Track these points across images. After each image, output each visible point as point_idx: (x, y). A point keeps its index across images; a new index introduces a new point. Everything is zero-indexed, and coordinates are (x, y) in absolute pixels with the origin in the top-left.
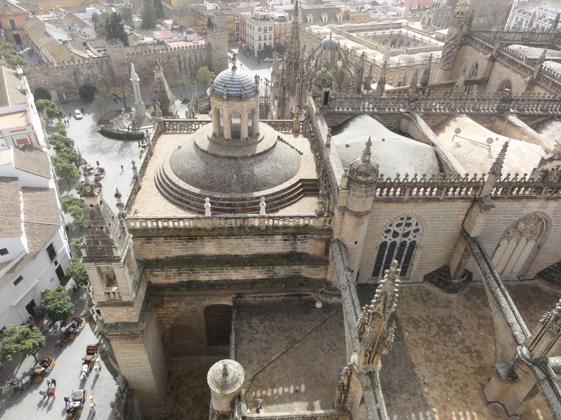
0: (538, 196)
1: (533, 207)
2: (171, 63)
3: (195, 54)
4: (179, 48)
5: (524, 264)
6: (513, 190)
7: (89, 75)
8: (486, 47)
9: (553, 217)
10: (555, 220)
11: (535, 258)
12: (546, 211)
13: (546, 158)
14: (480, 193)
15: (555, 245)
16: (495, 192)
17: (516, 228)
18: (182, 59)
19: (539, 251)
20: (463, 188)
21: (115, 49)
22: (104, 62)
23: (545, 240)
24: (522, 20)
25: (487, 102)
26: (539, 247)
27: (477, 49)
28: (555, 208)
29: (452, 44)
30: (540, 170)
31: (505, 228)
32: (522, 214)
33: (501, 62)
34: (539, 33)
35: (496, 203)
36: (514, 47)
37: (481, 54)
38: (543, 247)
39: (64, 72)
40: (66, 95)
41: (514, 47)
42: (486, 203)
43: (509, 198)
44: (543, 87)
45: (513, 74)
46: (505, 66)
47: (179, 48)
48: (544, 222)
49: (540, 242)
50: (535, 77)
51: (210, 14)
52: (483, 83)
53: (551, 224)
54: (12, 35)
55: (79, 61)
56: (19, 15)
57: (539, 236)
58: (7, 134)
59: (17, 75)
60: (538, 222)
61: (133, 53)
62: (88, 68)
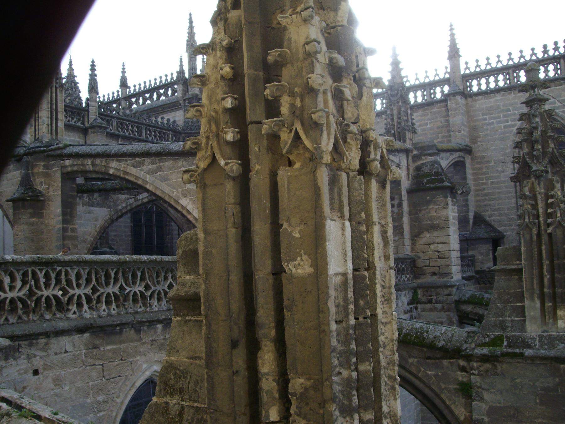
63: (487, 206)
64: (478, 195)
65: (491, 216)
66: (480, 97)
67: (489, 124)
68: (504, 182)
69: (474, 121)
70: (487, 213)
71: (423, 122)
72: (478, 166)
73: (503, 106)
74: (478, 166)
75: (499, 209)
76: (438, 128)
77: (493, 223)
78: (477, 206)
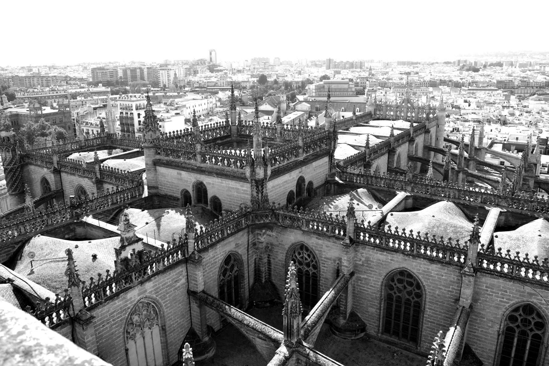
0: (132, 285)
1: (134, 295)
5: (162, 352)
6: (105, 291)
8: (46, 162)
9: (157, 296)
10: (160, 298)
11: (167, 342)
12: (147, 294)
13: (118, 248)
14: (74, 310)
15: (175, 320)
16: (89, 302)
17: (132, 324)
19: (166, 332)
20: (52, 315)
23: (164, 320)
24: (88, 130)
25: (58, 214)
26: (163, 329)
27: (39, 166)
28: (153, 287)
29: (12, 169)
30: (119, 261)
31: (122, 330)
32: (129, 308)
33: (66, 172)
34: (92, 139)
35: (94, 313)
36: (74, 156)
37: (45, 170)
38: (167, 327)
41: (74, 156)
42: (84, 318)
43: (106, 300)
44: (110, 183)
45: (81, 179)
46: (71, 174)
48: (153, 304)
49: (161, 324)
50: (99, 176)
52: (60, 194)
53: (160, 304)
57: (157, 319)
60: (148, 307)
63: (475, 342)
64: (470, 334)
65: (477, 349)
66: (487, 275)
67: (489, 295)
68: (491, 334)
69: (478, 288)
70: (474, 347)
71: (440, 273)
72: (474, 317)
73: (503, 287)
74: (474, 317)
75: (482, 348)
76: (451, 281)
77: (477, 354)
78: (467, 340)
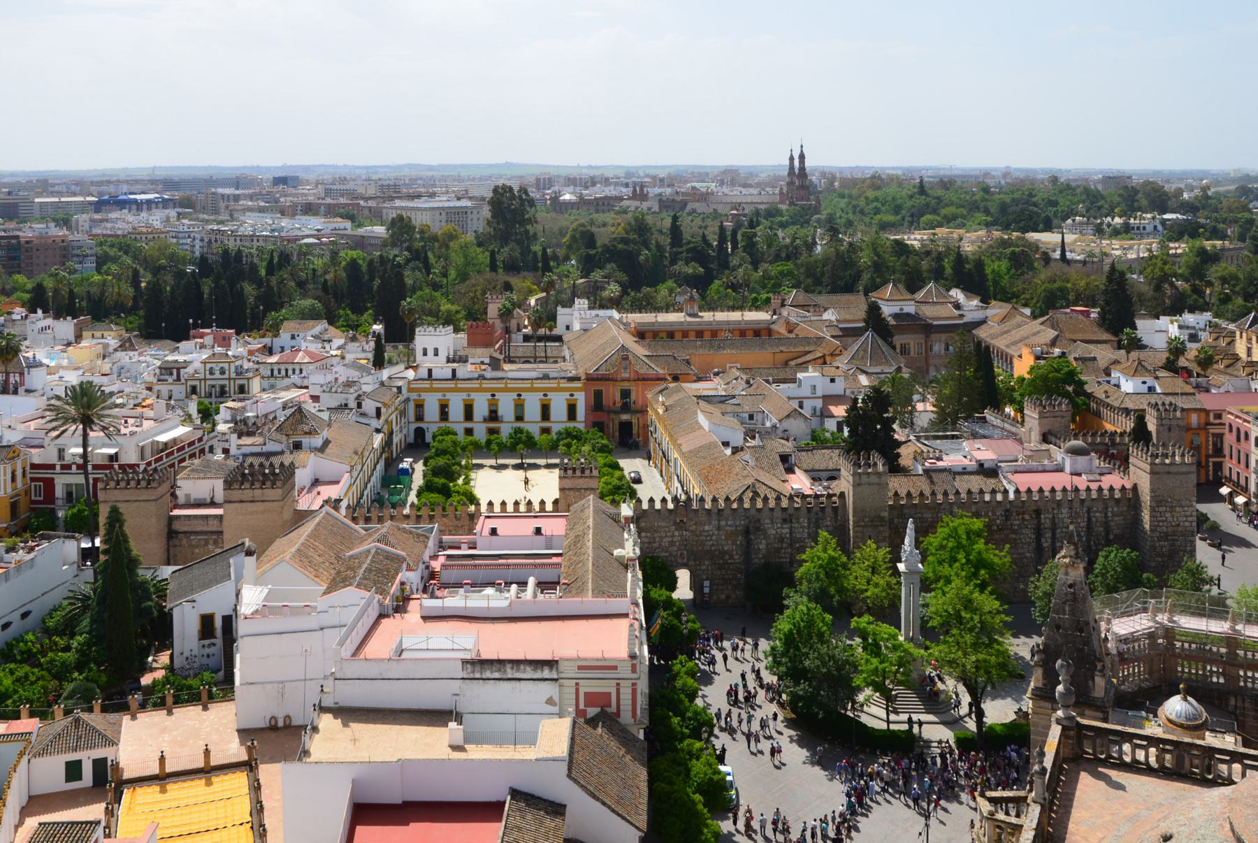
2: (1013, 532)
3: (1089, 511)
4: (1041, 490)
7: (781, 540)
18: (1048, 524)
21: (865, 479)
22: (829, 510)
39: (723, 523)
40: (711, 587)
47: (1041, 490)
51: (1131, 406)
54: (617, 422)
55: (766, 499)
56: (644, 379)
58: (568, 670)
59: (615, 519)
61: (909, 495)
62: (785, 521)
